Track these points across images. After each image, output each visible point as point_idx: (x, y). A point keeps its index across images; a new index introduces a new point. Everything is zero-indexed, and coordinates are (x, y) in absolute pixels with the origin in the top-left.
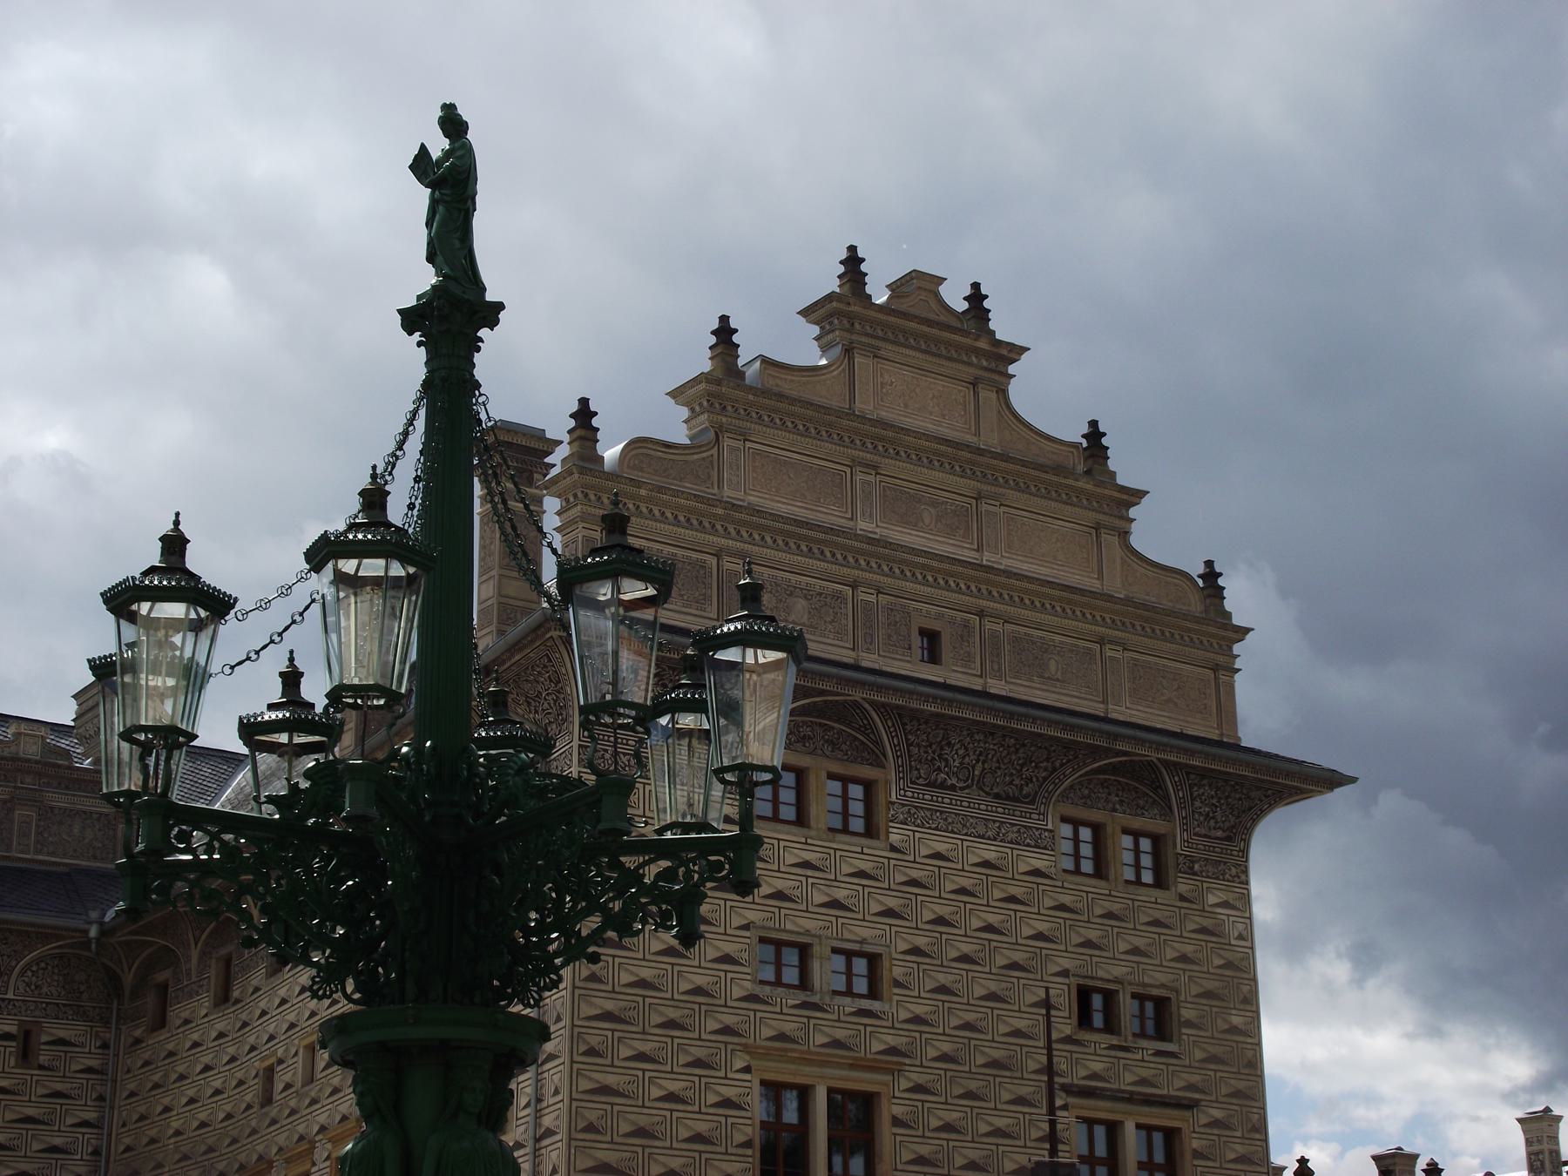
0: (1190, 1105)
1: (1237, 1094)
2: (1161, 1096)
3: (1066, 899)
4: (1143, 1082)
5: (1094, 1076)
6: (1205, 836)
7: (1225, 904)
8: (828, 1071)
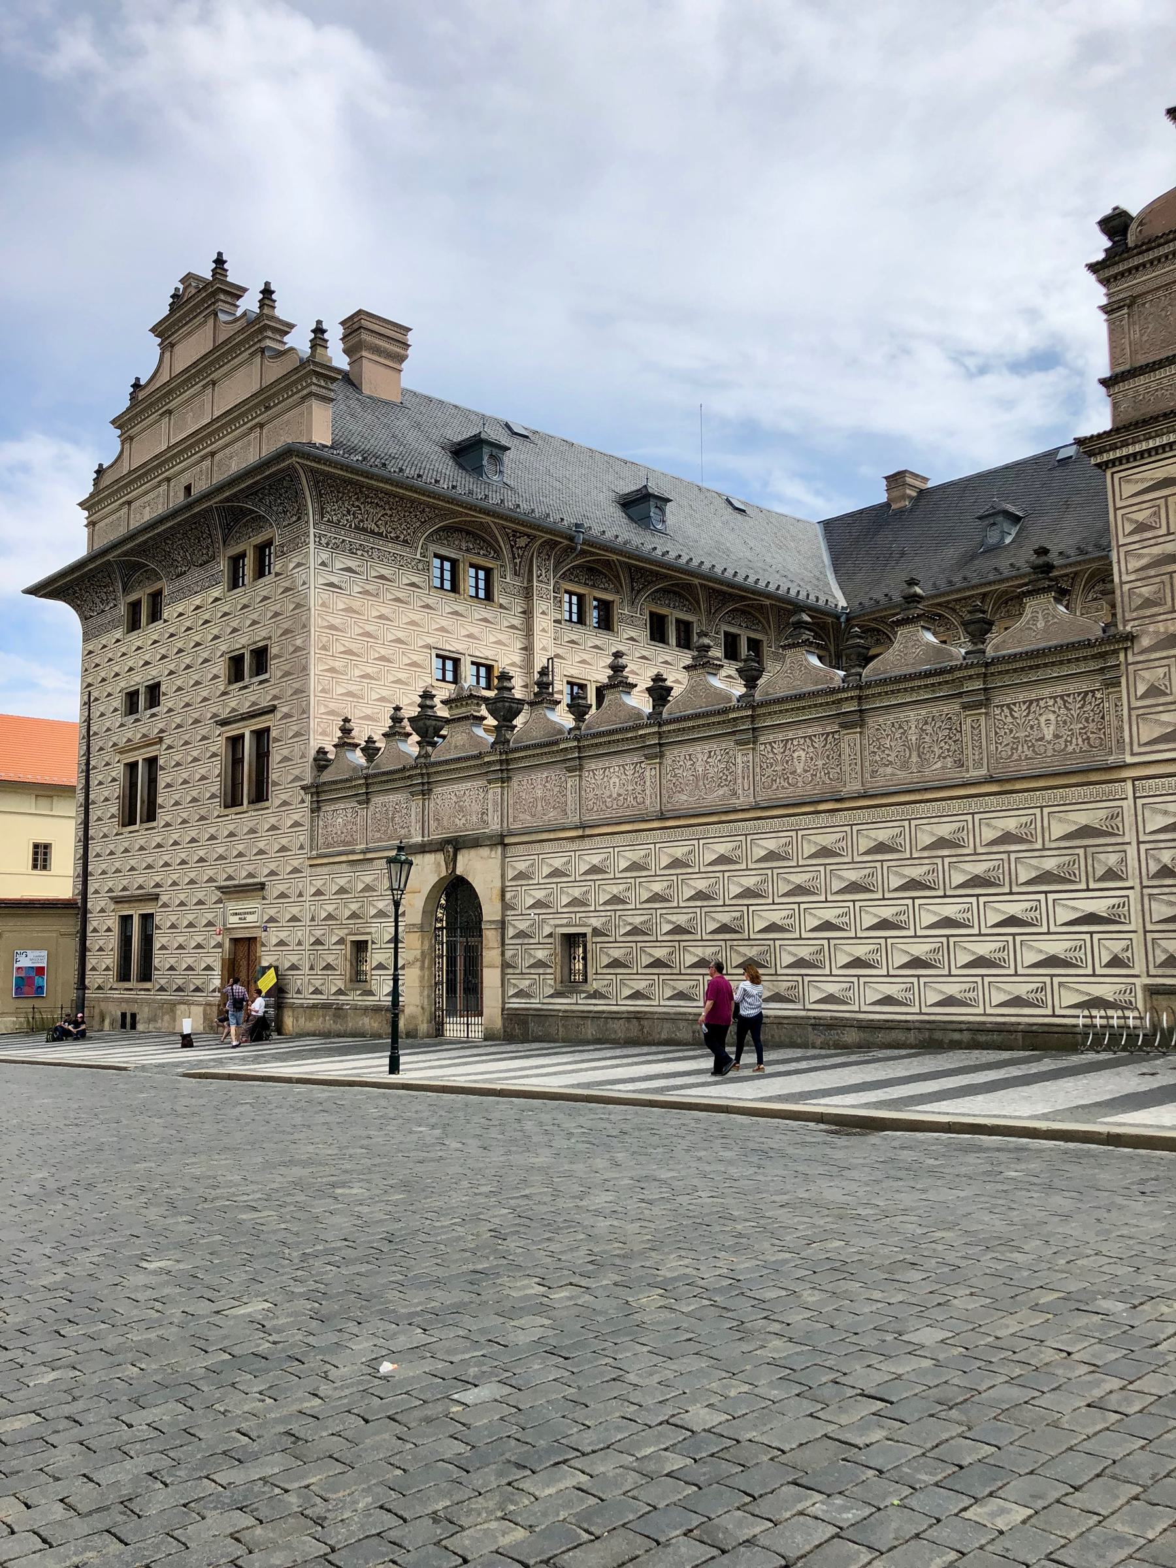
0: (272, 710)
1: (297, 692)
2: (259, 709)
3: (226, 609)
4: (254, 704)
5: (234, 710)
6: (289, 524)
7: (299, 565)
8: (142, 751)
